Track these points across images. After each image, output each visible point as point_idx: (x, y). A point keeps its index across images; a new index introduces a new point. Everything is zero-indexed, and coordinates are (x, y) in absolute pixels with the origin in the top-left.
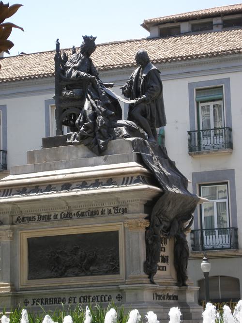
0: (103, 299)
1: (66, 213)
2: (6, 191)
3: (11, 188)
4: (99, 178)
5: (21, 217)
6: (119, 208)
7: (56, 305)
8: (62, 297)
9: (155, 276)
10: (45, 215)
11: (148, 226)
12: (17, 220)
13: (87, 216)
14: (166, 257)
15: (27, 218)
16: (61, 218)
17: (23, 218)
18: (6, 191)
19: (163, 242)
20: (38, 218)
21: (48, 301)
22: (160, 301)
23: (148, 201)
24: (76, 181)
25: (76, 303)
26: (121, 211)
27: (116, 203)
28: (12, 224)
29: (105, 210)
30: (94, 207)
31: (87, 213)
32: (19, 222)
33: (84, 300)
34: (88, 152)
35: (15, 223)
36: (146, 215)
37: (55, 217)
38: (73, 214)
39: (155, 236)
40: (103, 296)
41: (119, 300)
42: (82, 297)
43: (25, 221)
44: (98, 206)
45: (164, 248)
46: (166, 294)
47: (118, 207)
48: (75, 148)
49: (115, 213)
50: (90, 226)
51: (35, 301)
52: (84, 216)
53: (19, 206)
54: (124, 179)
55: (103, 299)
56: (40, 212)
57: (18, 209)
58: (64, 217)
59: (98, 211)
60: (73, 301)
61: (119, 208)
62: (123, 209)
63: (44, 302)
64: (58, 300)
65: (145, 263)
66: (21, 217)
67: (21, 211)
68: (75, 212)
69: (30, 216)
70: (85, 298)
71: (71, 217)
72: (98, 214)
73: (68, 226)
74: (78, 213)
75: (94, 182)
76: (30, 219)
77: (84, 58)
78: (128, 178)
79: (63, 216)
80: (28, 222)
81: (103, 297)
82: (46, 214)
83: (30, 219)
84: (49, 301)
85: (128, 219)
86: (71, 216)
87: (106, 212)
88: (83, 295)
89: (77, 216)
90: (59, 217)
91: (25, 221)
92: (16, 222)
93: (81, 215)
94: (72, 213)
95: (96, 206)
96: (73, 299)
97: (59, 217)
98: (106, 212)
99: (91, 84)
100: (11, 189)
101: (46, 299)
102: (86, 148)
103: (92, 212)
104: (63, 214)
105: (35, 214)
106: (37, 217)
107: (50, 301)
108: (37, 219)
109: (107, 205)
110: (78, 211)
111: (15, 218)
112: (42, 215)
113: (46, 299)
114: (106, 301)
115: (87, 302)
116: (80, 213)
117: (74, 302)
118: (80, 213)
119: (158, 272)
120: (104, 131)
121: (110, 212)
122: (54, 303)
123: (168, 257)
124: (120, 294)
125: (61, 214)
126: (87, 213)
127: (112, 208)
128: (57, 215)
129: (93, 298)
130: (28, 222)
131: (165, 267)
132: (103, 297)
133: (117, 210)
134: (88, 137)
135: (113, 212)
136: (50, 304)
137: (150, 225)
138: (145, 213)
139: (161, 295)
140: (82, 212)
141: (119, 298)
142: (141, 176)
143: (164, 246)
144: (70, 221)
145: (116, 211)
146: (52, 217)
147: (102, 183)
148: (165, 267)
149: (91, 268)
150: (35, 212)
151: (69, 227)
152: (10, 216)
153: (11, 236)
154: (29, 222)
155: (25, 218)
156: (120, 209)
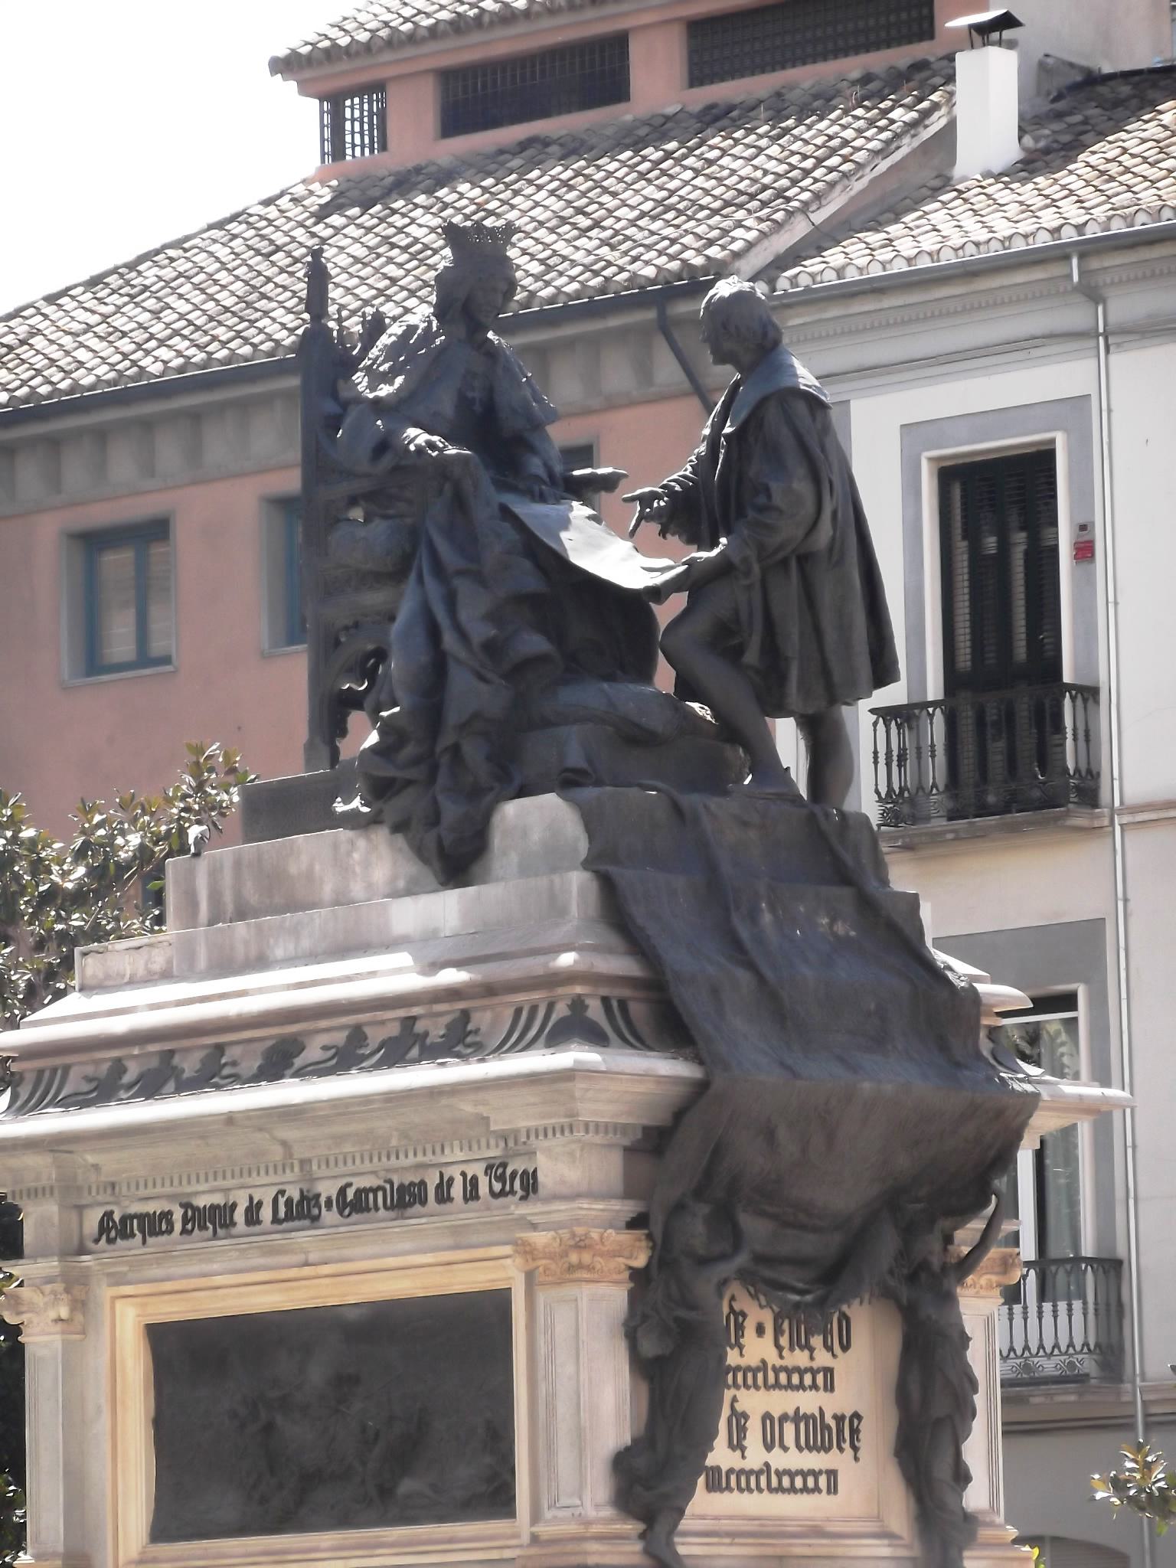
1: (296, 1197)
2: (47, 1074)
3: (58, 1061)
4: (416, 1011)
5: (117, 1217)
6: (509, 1171)
9: (685, 1524)
10: (212, 1206)
11: (640, 1261)
13: (382, 1211)
14: (839, 1419)
15: (141, 1217)
16: (276, 1220)
17: (125, 1219)
18: (47, 1074)
19: (817, 1341)
20: (185, 1220)
23: (647, 1130)
24: (323, 1024)
27: (492, 1142)
28: (82, 1251)
29: (451, 1180)
30: (404, 1162)
31: (380, 1194)
32: (110, 1241)
34: (410, 867)
35: (91, 1245)
36: (629, 1208)
37: (252, 1215)
38: (323, 1200)
39: (682, 1313)
43: (133, 1235)
44: (420, 1158)
45: (829, 1371)
47: (504, 1165)
48: (361, 843)
50: (391, 1262)
52: (368, 1210)
53: (91, 1159)
54: (518, 1012)
56: (189, 1189)
57: (93, 1177)
58: (289, 1217)
59: (423, 1184)
61: (509, 1171)
62: (525, 1172)
65: (622, 1463)
66: (117, 1217)
67: (113, 1185)
68: (327, 1189)
69: (151, 1207)
72: (424, 1202)
73: (307, 1264)
74: (342, 1192)
75: (394, 1030)
76: (154, 1225)
77: (443, 347)
78: (534, 1010)
80: (144, 1242)
82: (218, 1199)
83: (154, 1225)
85: (534, 1227)
87: (457, 1191)
89: (341, 1213)
90: (266, 1213)
91: (133, 1235)
92: (97, 1241)
93: (354, 1204)
94: (318, 1196)
95: (411, 1160)
97: (266, 1213)
98: (457, 1191)
99: (448, 487)
100: (66, 1069)
102: (400, 840)
103: (401, 1187)
104: (282, 1201)
105: (171, 1197)
106: (178, 1215)
108: (178, 1227)
109: (460, 1156)
110: (342, 1182)
111: (92, 1219)
112: (201, 1202)
116: (350, 1194)
118: (350, 1194)
119: (703, 1504)
120: (474, 752)
121: (471, 1192)
123: (856, 1416)
125: (275, 1201)
126: (380, 1194)
127: (477, 1169)
128: (260, 1204)
130: (144, 1242)
131: (832, 1474)
134: (409, 783)
135: (483, 1189)
137: (651, 1258)
138: (628, 1194)
140: (358, 1192)
142: (605, 1001)
143: (823, 1358)
144: (304, 1238)
145: (497, 1187)
146: (239, 1216)
147: (426, 1034)
148: (832, 1474)
149: (406, 1486)
150: (168, 1190)
151: (307, 1271)
152: (63, 1207)
153: (64, 1312)
154: (150, 1240)
155: (132, 1217)
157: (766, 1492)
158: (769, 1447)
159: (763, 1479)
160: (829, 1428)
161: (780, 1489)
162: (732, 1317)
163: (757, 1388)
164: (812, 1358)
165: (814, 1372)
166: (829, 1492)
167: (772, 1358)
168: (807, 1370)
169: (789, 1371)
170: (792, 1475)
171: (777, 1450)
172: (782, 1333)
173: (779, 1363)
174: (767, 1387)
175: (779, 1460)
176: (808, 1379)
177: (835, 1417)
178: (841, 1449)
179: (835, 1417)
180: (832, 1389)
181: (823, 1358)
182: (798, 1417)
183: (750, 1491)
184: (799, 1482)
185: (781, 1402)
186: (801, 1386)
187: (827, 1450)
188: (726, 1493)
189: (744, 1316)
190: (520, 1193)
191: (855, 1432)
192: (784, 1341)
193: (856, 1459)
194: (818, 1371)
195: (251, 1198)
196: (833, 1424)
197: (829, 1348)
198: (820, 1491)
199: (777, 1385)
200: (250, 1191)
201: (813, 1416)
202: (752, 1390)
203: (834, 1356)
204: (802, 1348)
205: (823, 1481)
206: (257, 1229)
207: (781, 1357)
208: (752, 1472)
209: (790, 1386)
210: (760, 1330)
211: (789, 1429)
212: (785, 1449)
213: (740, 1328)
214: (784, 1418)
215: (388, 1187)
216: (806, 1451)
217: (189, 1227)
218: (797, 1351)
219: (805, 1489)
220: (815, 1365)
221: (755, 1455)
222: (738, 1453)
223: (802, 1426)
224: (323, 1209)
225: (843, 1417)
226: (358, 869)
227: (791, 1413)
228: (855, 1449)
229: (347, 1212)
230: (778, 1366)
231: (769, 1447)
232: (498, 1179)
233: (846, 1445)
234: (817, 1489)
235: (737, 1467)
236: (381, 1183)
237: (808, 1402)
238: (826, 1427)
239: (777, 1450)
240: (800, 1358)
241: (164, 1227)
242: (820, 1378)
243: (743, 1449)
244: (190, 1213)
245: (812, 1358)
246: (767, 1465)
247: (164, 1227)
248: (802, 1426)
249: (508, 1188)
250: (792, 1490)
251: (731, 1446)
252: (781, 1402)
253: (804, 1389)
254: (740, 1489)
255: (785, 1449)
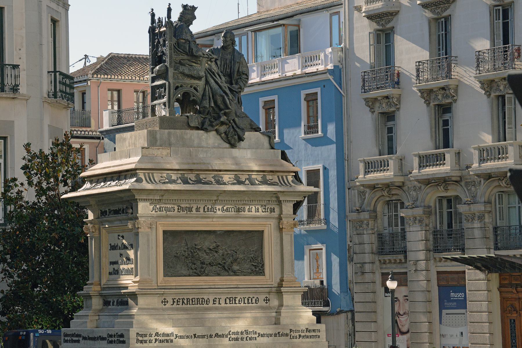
0: (250, 301)
6: (266, 207)
7: (199, 305)
8: (206, 298)
12: (153, 209)
21: (189, 301)
25: (221, 304)
26: (269, 210)
31: (233, 209)
33: (230, 301)
40: (250, 298)
41: (267, 303)
42: (228, 298)
49: (263, 212)
51: (175, 300)
55: (250, 301)
60: (217, 302)
61: (266, 207)
63: (185, 301)
64: (201, 300)
70: (231, 299)
71: (216, 212)
79: (206, 210)
81: (250, 299)
84: (191, 301)
86: (215, 211)
88: (229, 297)
96: (217, 300)
101: (187, 299)
104: (206, 208)
106: (176, 208)
107: (192, 302)
108: (176, 210)
113: (187, 299)
114: (253, 303)
115: (233, 303)
117: (219, 304)
122: (197, 304)
124: (268, 296)
125: (204, 208)
126: (233, 209)
129: (239, 300)
132: (250, 299)
133: (265, 209)
136: (193, 304)
141: (267, 300)
145: (264, 210)
146: (194, 210)
156: (268, 208)
190: (269, 212)
195: (197, 206)
200: (197, 205)
206: (199, 213)
215: (235, 207)
217: (180, 211)
224: (217, 210)
226: (204, 140)
229: (224, 212)
232: (264, 209)
236: (233, 207)
241: (172, 210)
244: (180, 208)
247: (172, 210)
249: (266, 211)
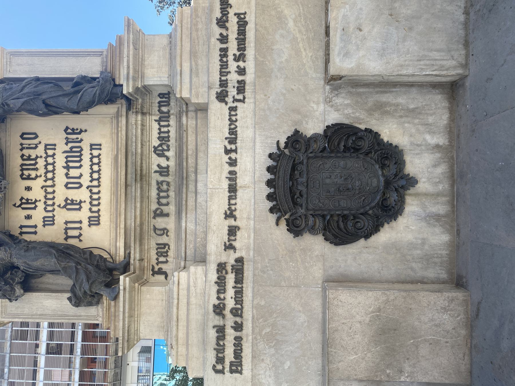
19: (33, 153)
22: (172, 194)
46: (156, 161)
131: (92, 147)
139: (158, 183)
143: (40, 151)
148: (92, 147)
157: (100, 189)
158: (81, 186)
159: (95, 190)
160: (72, 148)
161: (98, 179)
162: (23, 206)
163: (54, 192)
164: (41, 157)
165: (48, 156)
166: (100, 149)
167: (40, 182)
168: (46, 161)
169: (47, 172)
170: (93, 172)
171: (81, 181)
172: (29, 175)
173: (43, 178)
174: (53, 186)
175: (85, 181)
176: (50, 160)
177: (66, 144)
178: (82, 140)
179: (66, 144)
180: (55, 145)
181: (40, 151)
182: (68, 168)
183: (99, 198)
184: (95, 168)
185: (61, 179)
186: (53, 164)
187: (82, 150)
188: (100, 213)
189: (22, 198)
191: (74, 132)
192: (33, 174)
193: (86, 131)
194: (46, 153)
196: (70, 145)
197: (36, 147)
198: (100, 155)
199: (52, 179)
201: (67, 157)
202: (55, 195)
203: (40, 143)
204: (36, 163)
205: (95, 153)
207: (41, 176)
208: (91, 197)
209: (53, 171)
210: (28, 189)
211: (73, 173)
212: (81, 175)
213: (28, 202)
214: (67, 175)
216: (82, 163)
218: (37, 166)
219: (98, 164)
220: (44, 155)
221: (83, 195)
222: (82, 204)
223: (71, 164)
225: (67, 138)
227: (65, 171)
228: (81, 131)
230: (45, 179)
231: (81, 186)
233: (79, 136)
234: (99, 156)
235: (89, 206)
237: (60, 160)
238: (71, 151)
239: (81, 181)
240: (41, 163)
242: (50, 152)
243: (81, 202)
245: (41, 157)
246: (88, 188)
248: (71, 164)
250: (99, 171)
251: (79, 209)
252: (61, 179)
253: (54, 162)
254: (99, 204)
255: (81, 175)
